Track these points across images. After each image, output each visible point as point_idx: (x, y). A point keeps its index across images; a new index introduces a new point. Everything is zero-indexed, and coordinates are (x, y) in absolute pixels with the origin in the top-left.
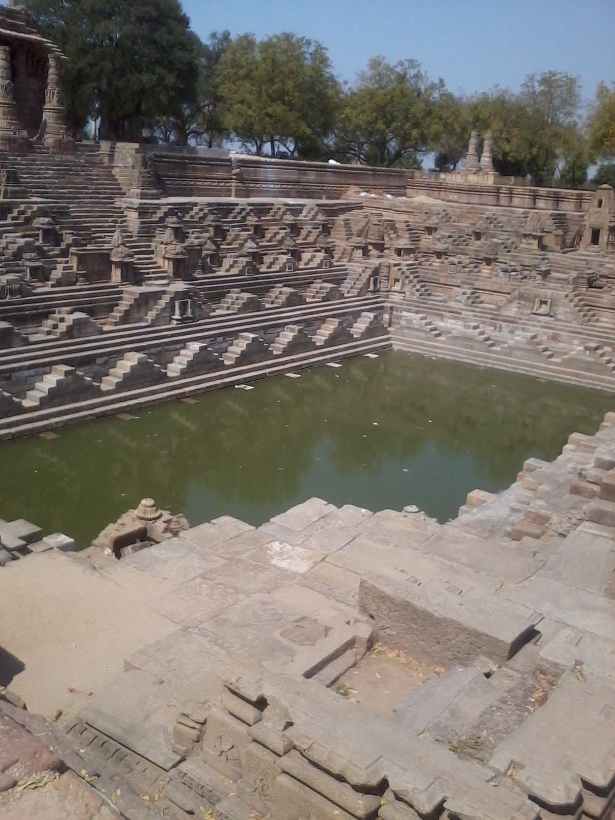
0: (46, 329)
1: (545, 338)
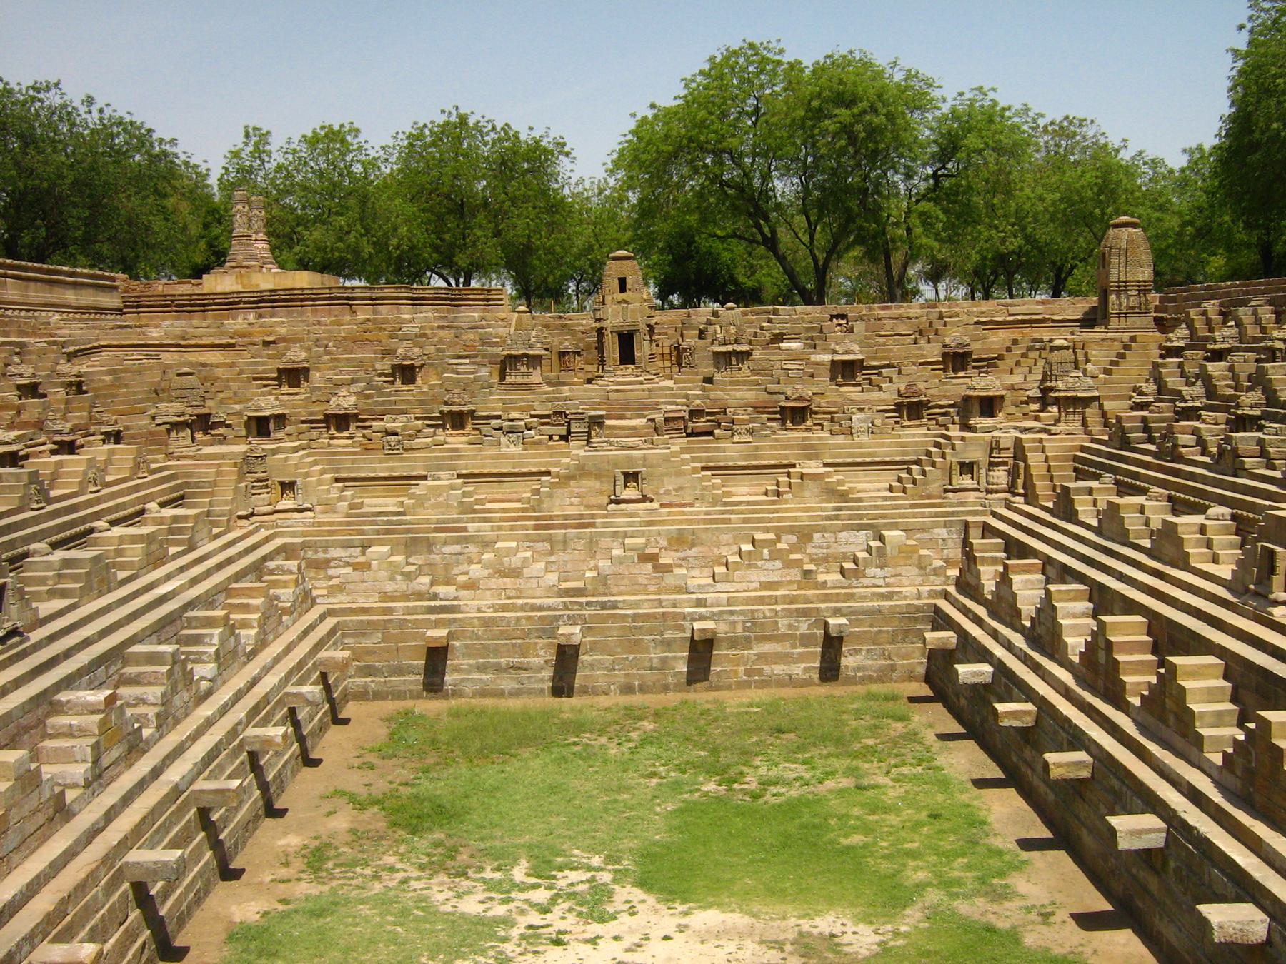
1: (663, 543)
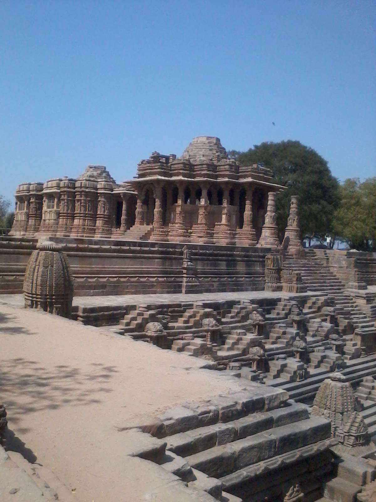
0: (365, 396)
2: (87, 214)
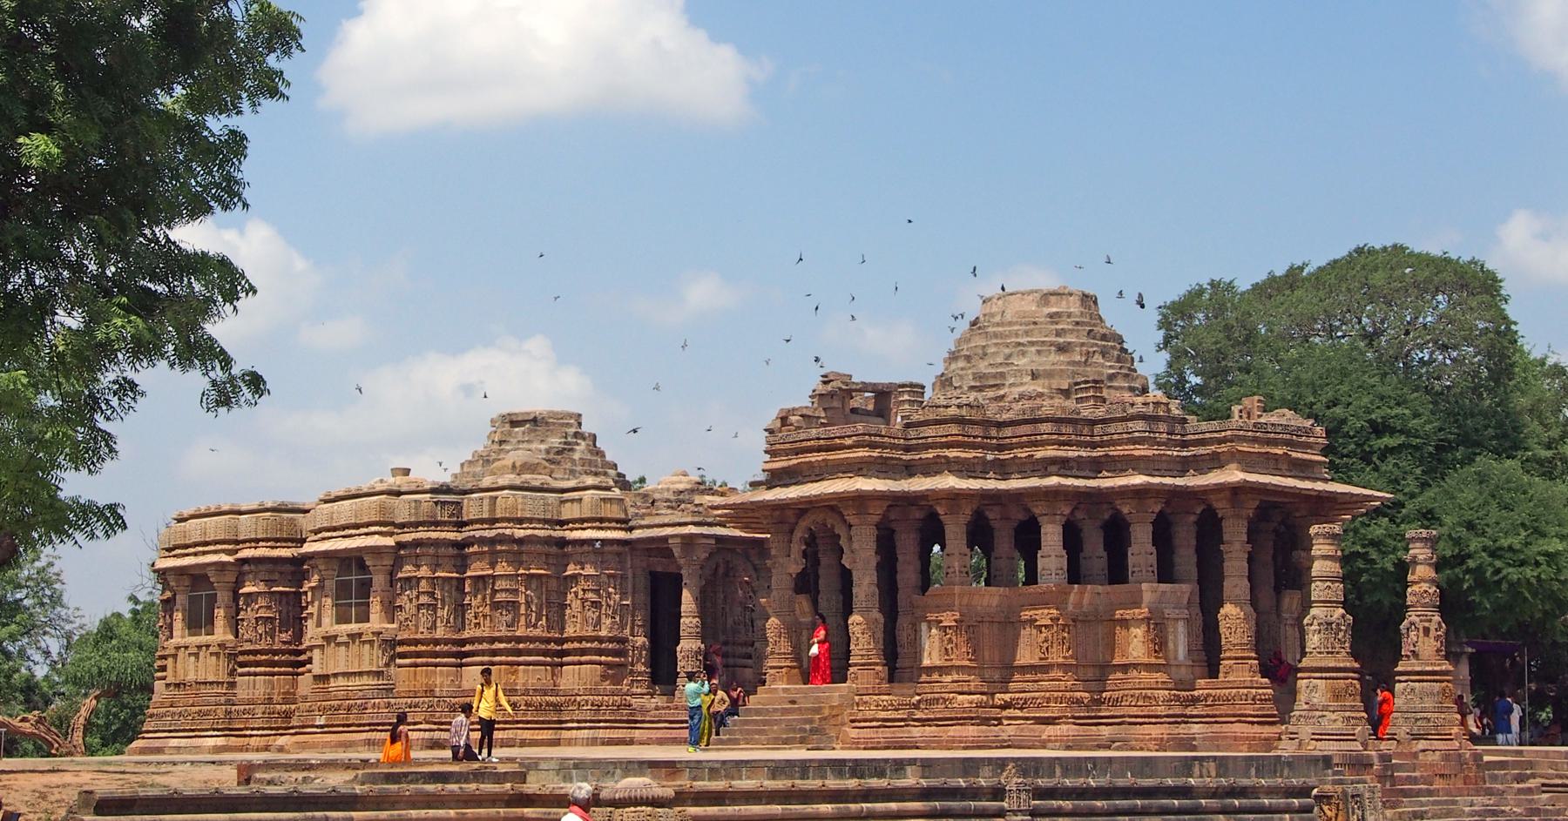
2: (519, 640)
